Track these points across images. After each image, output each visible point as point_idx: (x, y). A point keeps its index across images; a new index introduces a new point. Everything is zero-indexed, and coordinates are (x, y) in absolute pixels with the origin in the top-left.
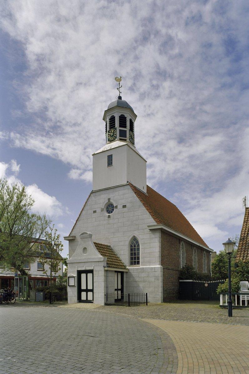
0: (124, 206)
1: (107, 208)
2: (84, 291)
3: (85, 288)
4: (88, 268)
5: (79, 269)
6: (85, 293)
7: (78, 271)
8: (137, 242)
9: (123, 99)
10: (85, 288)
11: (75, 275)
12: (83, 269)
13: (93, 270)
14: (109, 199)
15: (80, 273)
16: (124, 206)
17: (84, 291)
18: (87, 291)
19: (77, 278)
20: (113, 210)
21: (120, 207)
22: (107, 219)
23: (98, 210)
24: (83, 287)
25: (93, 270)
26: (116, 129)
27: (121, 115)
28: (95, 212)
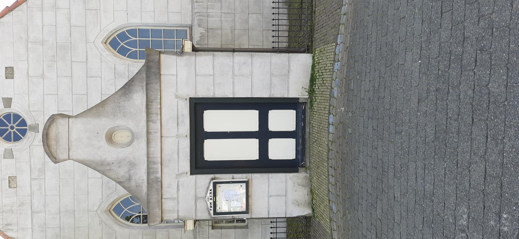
0: (10, 73)
2: (263, 149)
3: (255, 143)
5: (186, 165)
6: (273, 143)
7: (192, 174)
8: (122, 36)
10: (255, 143)
12: (186, 144)
16: (10, 73)
17: (263, 149)
19: (217, 176)
20: (17, 117)
28: (12, 181)
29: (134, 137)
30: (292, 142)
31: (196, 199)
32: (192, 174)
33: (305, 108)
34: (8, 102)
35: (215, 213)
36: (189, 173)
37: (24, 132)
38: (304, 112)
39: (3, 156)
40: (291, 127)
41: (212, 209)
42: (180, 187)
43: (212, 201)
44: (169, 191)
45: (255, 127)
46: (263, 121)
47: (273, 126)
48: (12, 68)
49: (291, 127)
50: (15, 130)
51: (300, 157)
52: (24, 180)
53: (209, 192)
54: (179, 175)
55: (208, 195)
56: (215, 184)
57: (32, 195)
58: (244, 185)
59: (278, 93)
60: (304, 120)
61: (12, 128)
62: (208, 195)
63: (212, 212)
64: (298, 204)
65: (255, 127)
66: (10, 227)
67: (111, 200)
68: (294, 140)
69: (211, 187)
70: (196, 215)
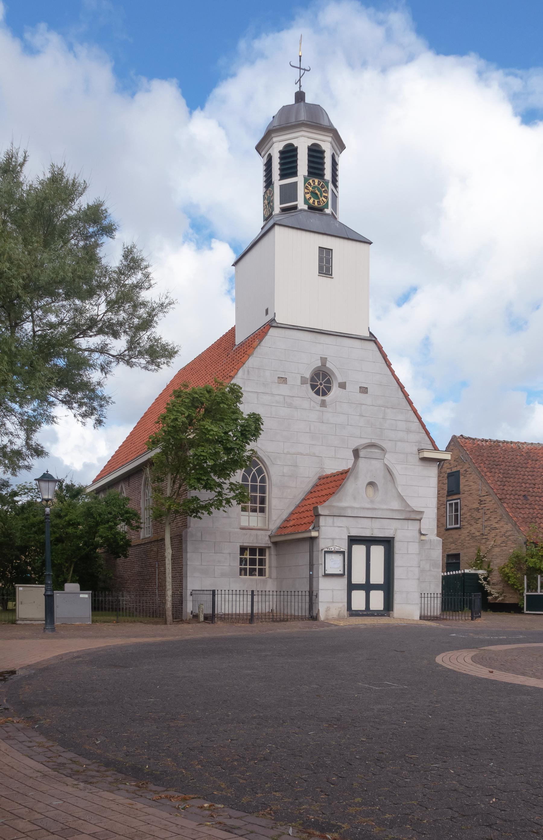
0: (364, 390)
1: (312, 379)
4: (378, 533)
7: (349, 536)
9: (309, 99)
11: (344, 547)
12: (367, 533)
13: (394, 538)
14: (324, 360)
15: (353, 540)
16: (364, 390)
18: (368, 587)
21: (353, 388)
22: (318, 408)
23: (294, 380)
24: (358, 577)
25: (394, 538)
26: (327, 183)
27: (314, 145)
28: (283, 380)
29: (372, 502)
30: (363, 607)
31: (333, 539)
32: (349, 536)
33: (386, 616)
34: (343, 386)
35: (326, 552)
36: (349, 535)
37: (317, 393)
38: (383, 615)
39: (303, 376)
40: (373, 607)
41: (328, 550)
42: (341, 528)
43: (333, 550)
44: (339, 521)
45: (373, 581)
46: (377, 587)
47: (373, 593)
48: (367, 393)
49: (373, 607)
50: (319, 386)
51: (354, 612)
52: (284, 390)
53: (339, 548)
54: (348, 528)
55: (337, 548)
56: (343, 553)
57: (273, 395)
58: (341, 572)
59: (397, 598)
60: (378, 615)
61: (321, 384)
62: (337, 548)
63: (326, 550)
64: (328, 609)
65: (373, 581)
66: (246, 372)
67: (265, 459)
68: (364, 609)
69: (342, 550)
70: (322, 538)
